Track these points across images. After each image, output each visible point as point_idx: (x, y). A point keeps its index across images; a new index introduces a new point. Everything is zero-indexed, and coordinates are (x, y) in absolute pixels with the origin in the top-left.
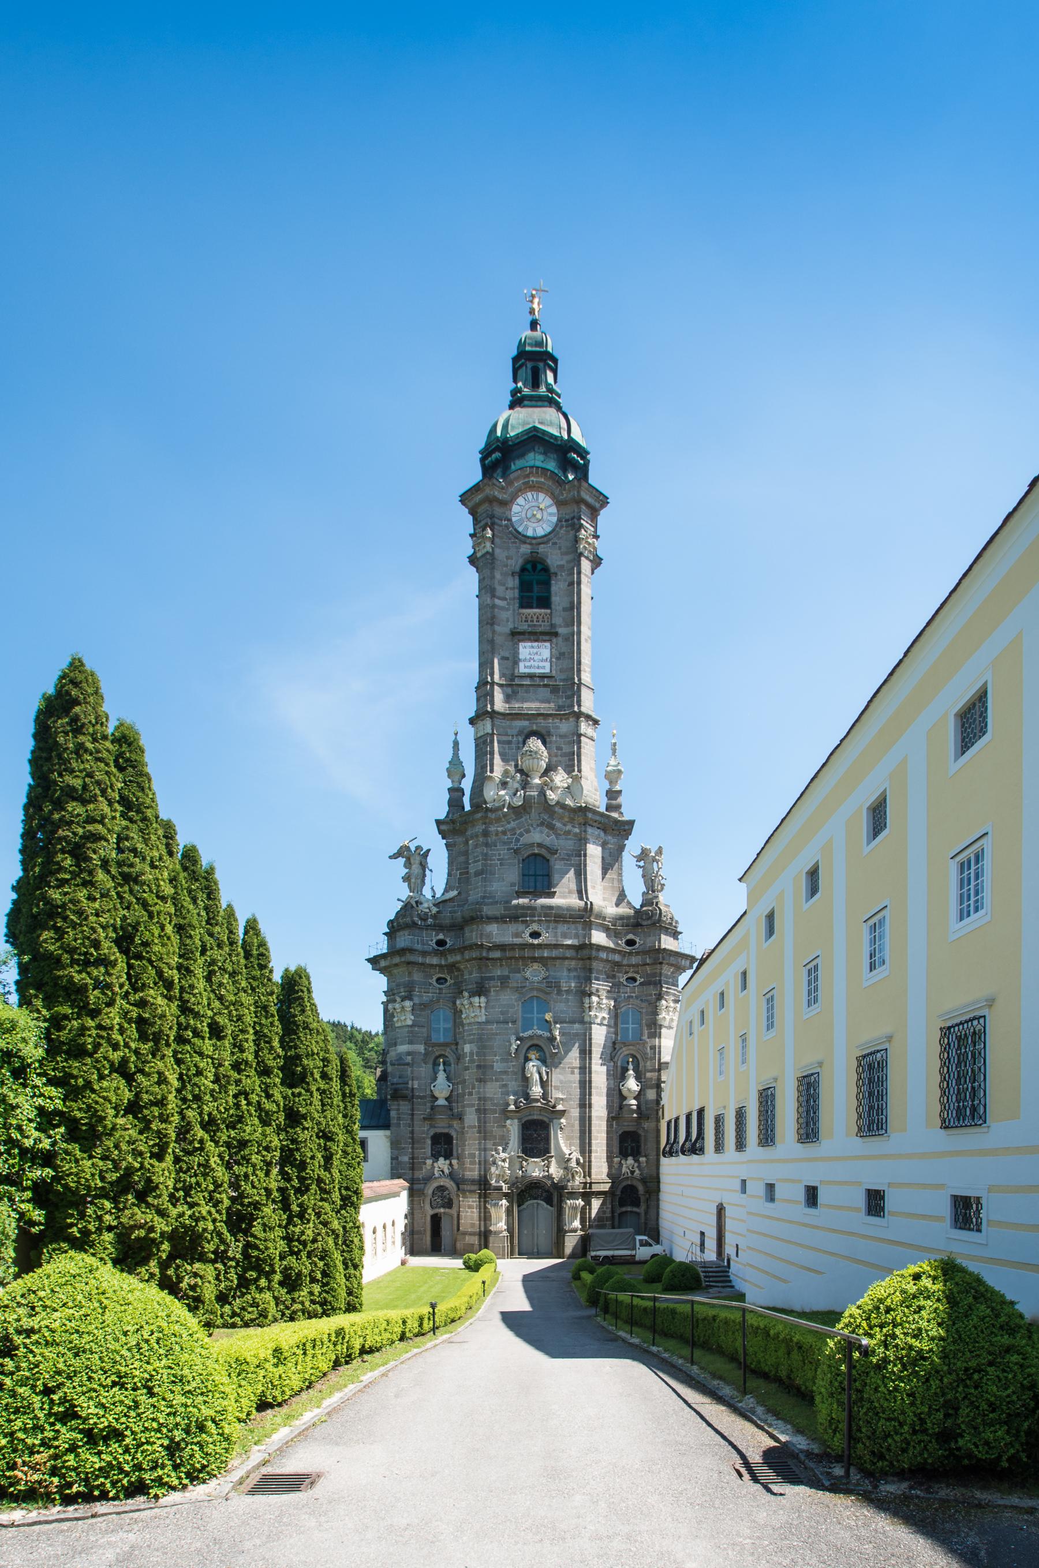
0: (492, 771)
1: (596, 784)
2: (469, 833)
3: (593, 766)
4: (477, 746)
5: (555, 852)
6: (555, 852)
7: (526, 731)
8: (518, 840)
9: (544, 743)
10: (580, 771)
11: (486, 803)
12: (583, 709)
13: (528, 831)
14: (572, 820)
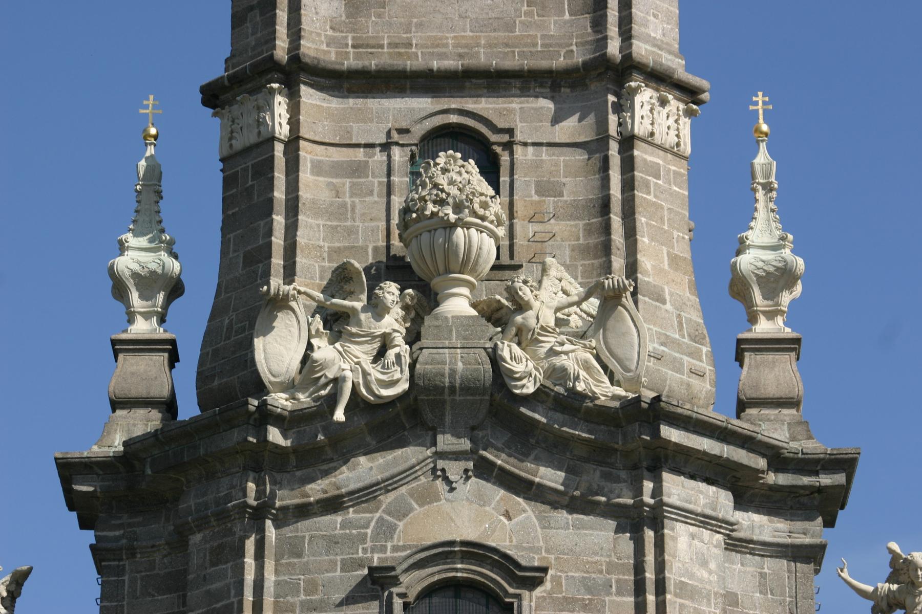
0: (290, 274)
1: (696, 317)
2: (190, 502)
3: (683, 250)
4: (228, 182)
5: (532, 578)
6: (532, 578)
7: (419, 130)
8: (386, 530)
9: (491, 171)
10: (632, 269)
11: (259, 388)
12: (641, 50)
13: (426, 497)
14: (599, 454)
